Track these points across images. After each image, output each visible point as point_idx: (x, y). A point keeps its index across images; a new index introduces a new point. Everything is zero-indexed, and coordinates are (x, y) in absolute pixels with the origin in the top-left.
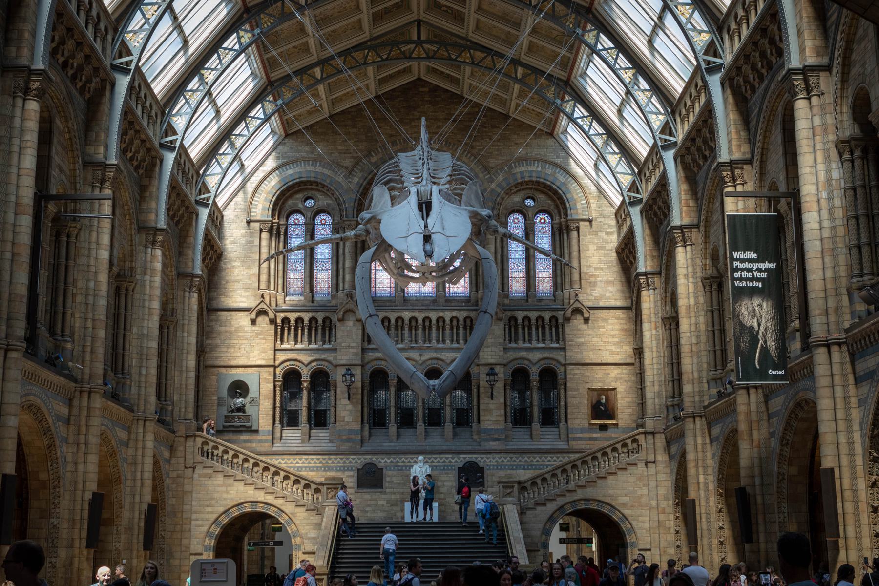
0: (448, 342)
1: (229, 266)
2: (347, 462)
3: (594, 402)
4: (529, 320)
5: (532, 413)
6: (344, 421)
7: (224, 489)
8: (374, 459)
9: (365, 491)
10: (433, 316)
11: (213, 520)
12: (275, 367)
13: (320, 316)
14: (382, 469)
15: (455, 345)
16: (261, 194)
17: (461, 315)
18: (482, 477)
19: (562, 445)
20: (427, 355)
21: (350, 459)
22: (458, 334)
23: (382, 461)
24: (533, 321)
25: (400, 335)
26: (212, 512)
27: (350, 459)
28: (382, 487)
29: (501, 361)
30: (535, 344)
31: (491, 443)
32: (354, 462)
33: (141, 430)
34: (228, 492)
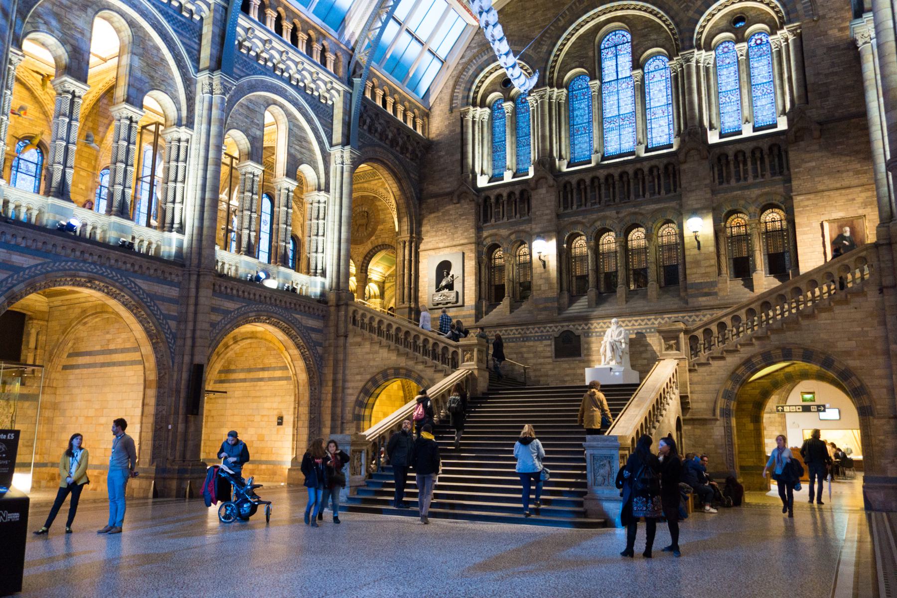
1: (436, 157)
2: (545, 331)
3: (834, 236)
6: (540, 289)
7: (371, 356)
9: (562, 359)
11: (360, 388)
14: (579, 336)
16: (460, 86)
21: (548, 328)
24: (748, 154)
25: (597, 196)
26: (361, 381)
27: (548, 328)
28: (580, 355)
31: (700, 299)
32: (551, 330)
33: (193, 285)
34: (374, 360)
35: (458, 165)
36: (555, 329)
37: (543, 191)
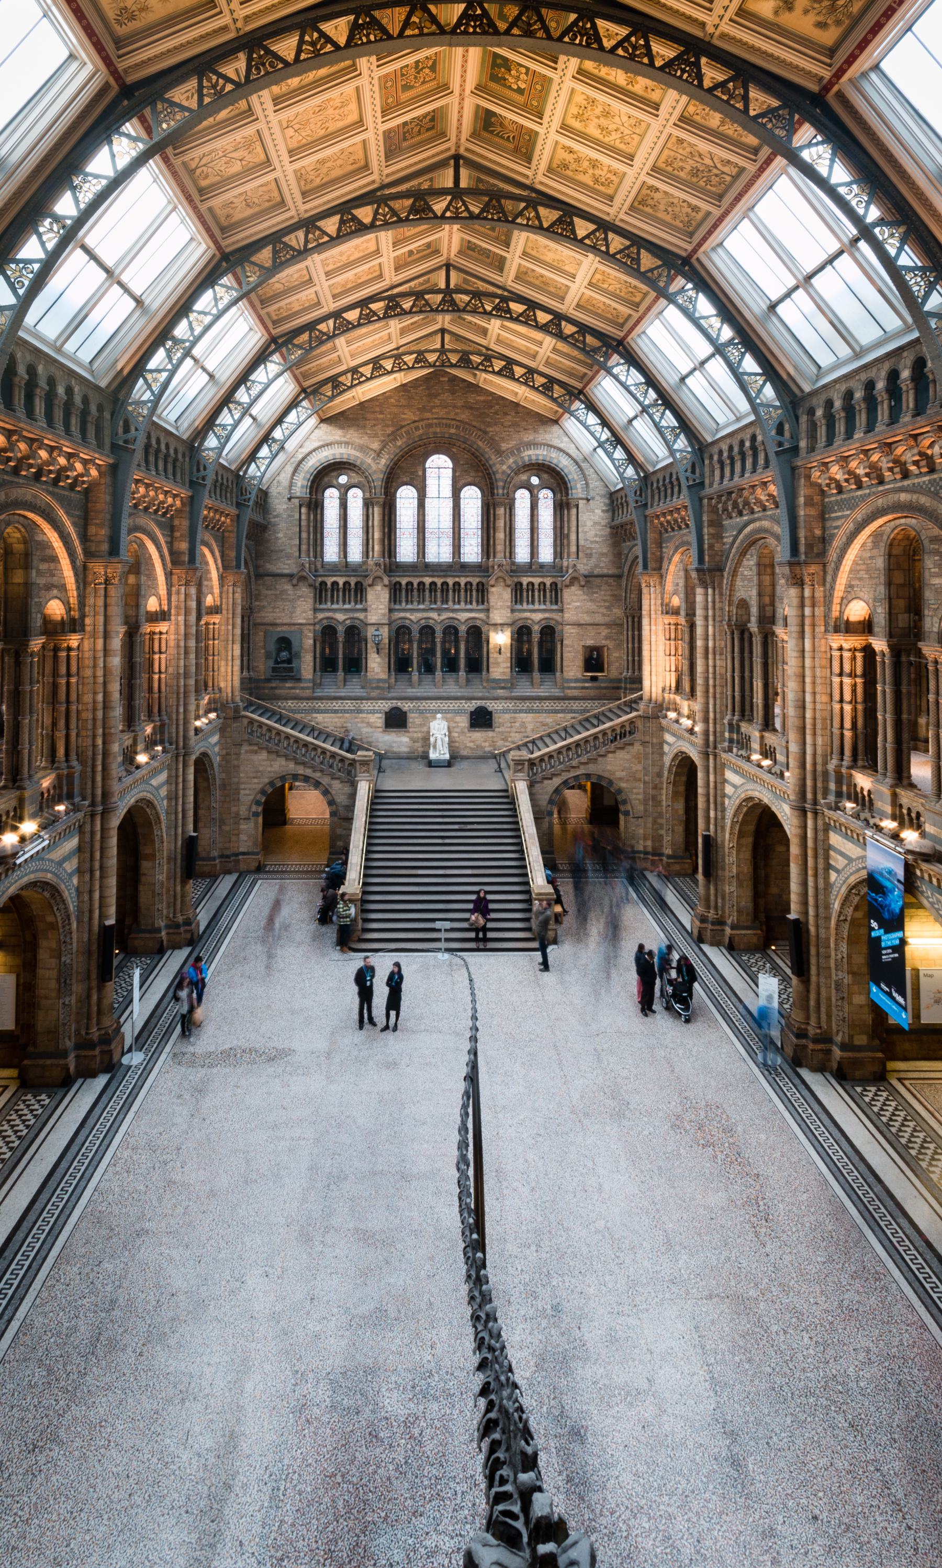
0: (463, 603)
4: (533, 584)
5: (532, 663)
8: (399, 704)
10: (450, 581)
12: (314, 624)
13: (353, 581)
15: (469, 607)
17: (474, 581)
18: (491, 719)
19: (556, 692)
20: (445, 615)
22: (471, 596)
23: (406, 706)
24: (536, 586)
29: (509, 621)
30: (537, 606)
33: (181, 766)
35: (296, 549)
36: (386, 705)
37: (379, 588)
